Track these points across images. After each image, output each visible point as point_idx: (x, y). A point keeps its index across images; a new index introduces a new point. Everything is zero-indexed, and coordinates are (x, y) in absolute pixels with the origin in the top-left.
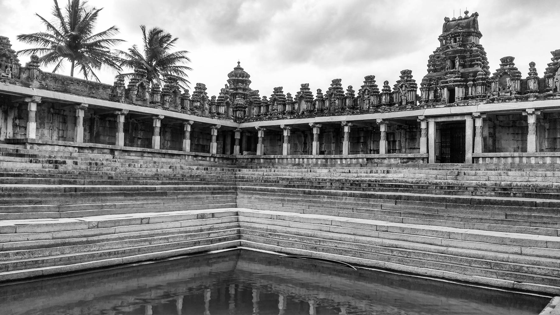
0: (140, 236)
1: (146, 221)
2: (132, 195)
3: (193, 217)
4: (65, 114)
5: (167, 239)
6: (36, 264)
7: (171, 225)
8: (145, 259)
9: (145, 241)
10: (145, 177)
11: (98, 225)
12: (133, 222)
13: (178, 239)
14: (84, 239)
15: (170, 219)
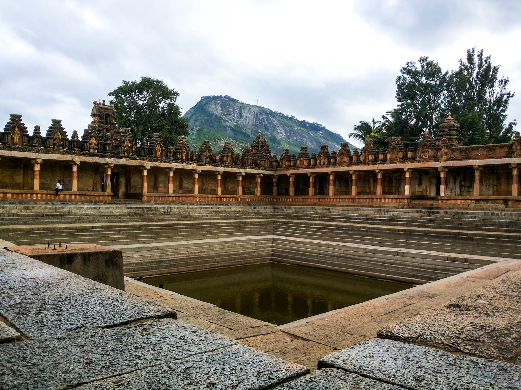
0: (384, 262)
1: (402, 254)
2: (437, 237)
3: (443, 258)
4: (498, 172)
5: (398, 268)
6: (322, 263)
7: (425, 261)
8: (367, 275)
9: (382, 265)
10: (494, 224)
11: (370, 251)
12: (392, 253)
13: (406, 270)
14: (353, 257)
15: (420, 257)
